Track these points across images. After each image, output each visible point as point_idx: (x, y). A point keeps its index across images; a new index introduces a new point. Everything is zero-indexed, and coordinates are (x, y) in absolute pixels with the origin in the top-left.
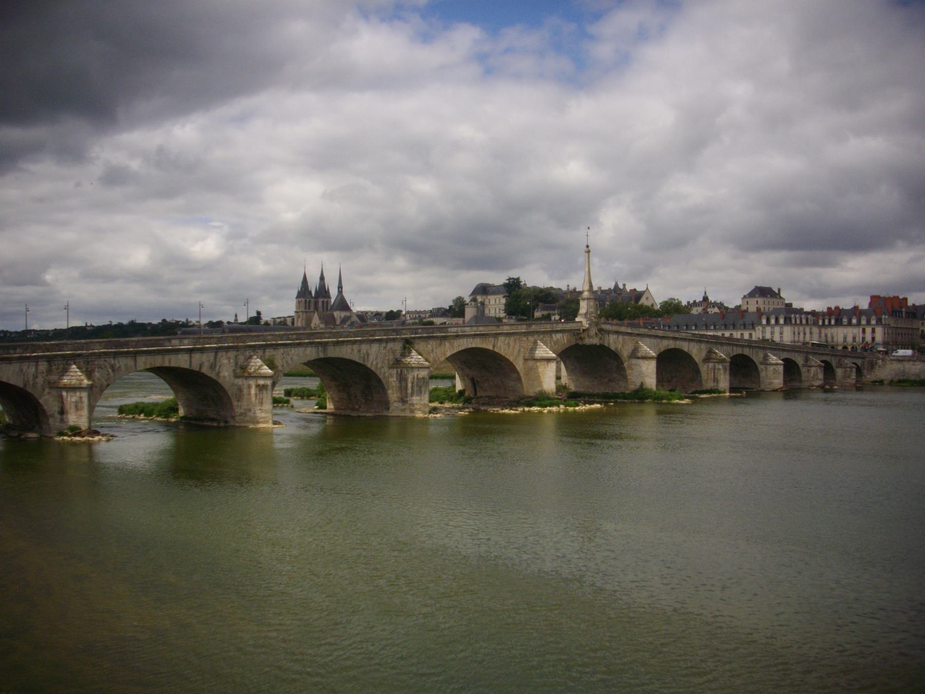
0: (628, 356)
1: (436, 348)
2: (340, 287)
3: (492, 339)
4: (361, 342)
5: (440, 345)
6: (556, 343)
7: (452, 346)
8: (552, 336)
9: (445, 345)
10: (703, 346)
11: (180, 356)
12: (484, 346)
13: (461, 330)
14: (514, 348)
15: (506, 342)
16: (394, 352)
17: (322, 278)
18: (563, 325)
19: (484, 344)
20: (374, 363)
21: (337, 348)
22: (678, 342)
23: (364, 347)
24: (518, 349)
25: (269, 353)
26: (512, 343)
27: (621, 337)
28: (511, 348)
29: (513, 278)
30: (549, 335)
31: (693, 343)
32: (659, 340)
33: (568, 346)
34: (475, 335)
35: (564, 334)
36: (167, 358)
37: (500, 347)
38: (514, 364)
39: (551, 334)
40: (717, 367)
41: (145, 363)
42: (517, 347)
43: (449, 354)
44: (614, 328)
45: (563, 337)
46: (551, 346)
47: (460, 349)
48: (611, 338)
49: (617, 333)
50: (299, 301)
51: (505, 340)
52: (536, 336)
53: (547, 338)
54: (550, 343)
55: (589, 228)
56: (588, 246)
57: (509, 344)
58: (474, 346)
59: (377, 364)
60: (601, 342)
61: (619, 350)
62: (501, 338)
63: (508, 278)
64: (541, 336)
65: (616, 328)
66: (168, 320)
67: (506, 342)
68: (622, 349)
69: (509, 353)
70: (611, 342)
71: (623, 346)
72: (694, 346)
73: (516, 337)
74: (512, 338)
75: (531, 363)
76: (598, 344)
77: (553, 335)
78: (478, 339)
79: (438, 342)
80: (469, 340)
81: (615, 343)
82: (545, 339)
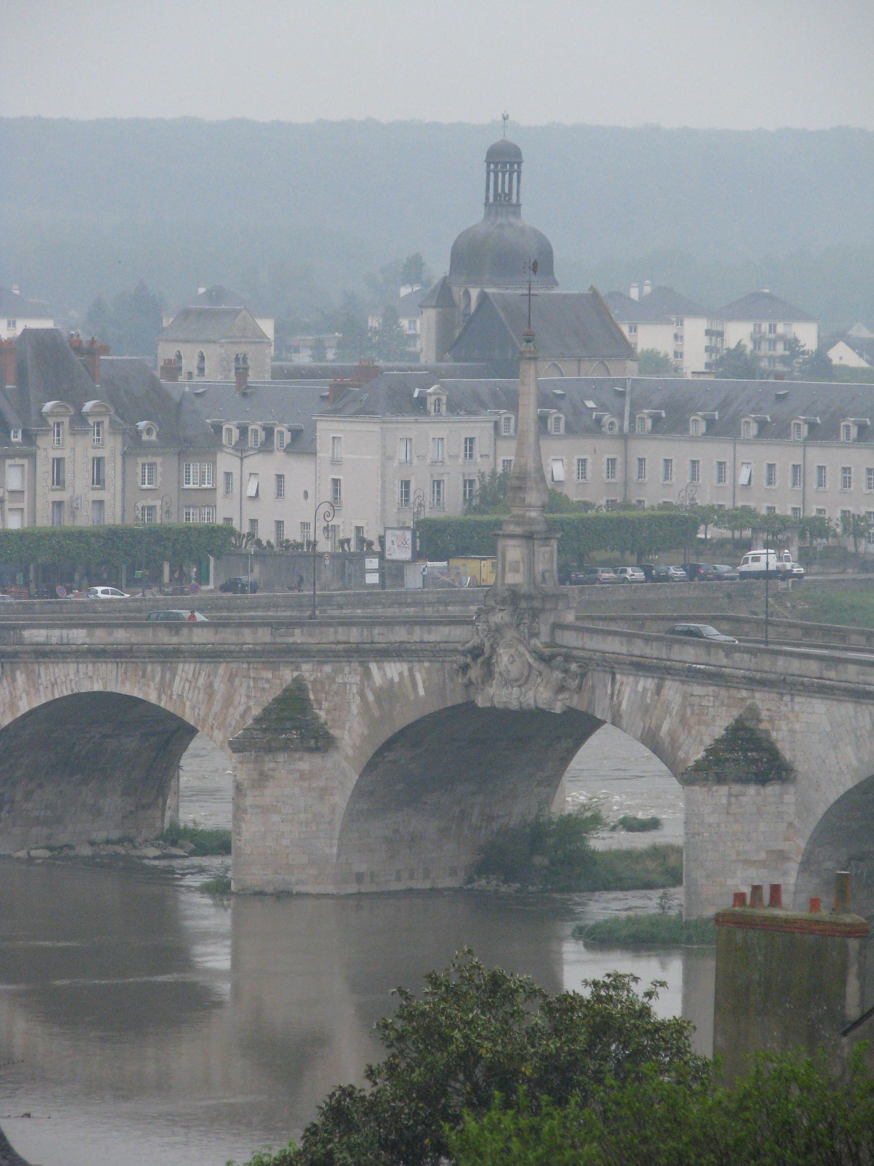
3: (155, 670)
6: (379, 694)
7: (33, 682)
9: (14, 680)
12: (130, 689)
13: (62, 638)
14: (228, 701)
15: (201, 681)
18: (410, 633)
19: (128, 684)
24: (242, 708)
26: (220, 687)
27: (672, 690)
30: (356, 665)
33: (431, 709)
34: (97, 654)
35: (417, 666)
37: (180, 696)
39: (364, 665)
43: (24, 707)
44: (639, 648)
45: (411, 670)
47: (57, 696)
48: (627, 690)
49: (640, 667)
51: (196, 676)
52: (307, 670)
58: (97, 687)
60: (576, 702)
61: (667, 740)
62: (185, 669)
64: (328, 669)
65: (648, 651)
67: (201, 681)
69: (210, 720)
70: (624, 706)
71: (683, 721)
73: (235, 665)
74: (222, 669)
76: (558, 709)
77: (373, 666)
78: (112, 667)
80: (82, 667)
81: (646, 710)
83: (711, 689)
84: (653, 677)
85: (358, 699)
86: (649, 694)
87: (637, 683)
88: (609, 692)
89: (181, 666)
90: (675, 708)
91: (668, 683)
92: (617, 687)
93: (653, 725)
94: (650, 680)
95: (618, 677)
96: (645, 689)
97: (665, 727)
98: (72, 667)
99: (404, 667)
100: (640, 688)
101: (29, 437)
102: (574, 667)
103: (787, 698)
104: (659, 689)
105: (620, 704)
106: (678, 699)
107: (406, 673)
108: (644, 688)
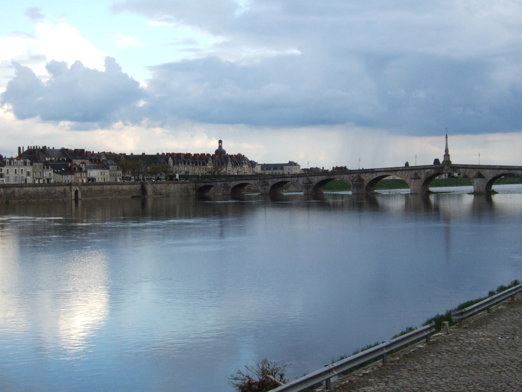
0: (473, 177)
1: (370, 176)
4: (341, 174)
5: (371, 175)
8: (425, 171)
11: (289, 179)
14: (405, 175)
16: (353, 177)
20: (346, 180)
21: (333, 176)
22: (512, 171)
23: (342, 176)
25: (313, 177)
26: (404, 174)
27: (468, 170)
28: (403, 175)
32: (496, 171)
36: (286, 179)
38: (405, 180)
41: (280, 180)
42: (406, 174)
43: (375, 177)
45: (431, 170)
46: (425, 174)
52: (416, 171)
53: (423, 171)
54: (424, 173)
57: (402, 174)
59: (347, 180)
64: (419, 171)
66: (338, 166)
67: (401, 173)
68: (469, 174)
71: (469, 173)
74: (404, 171)
75: (411, 180)
77: (426, 170)
79: (370, 173)
80: (383, 173)
82: (421, 172)
85: (423, 173)
89: (398, 172)
98: (382, 173)
99: (430, 170)
101: (242, 165)
102: (454, 168)
104: (466, 170)
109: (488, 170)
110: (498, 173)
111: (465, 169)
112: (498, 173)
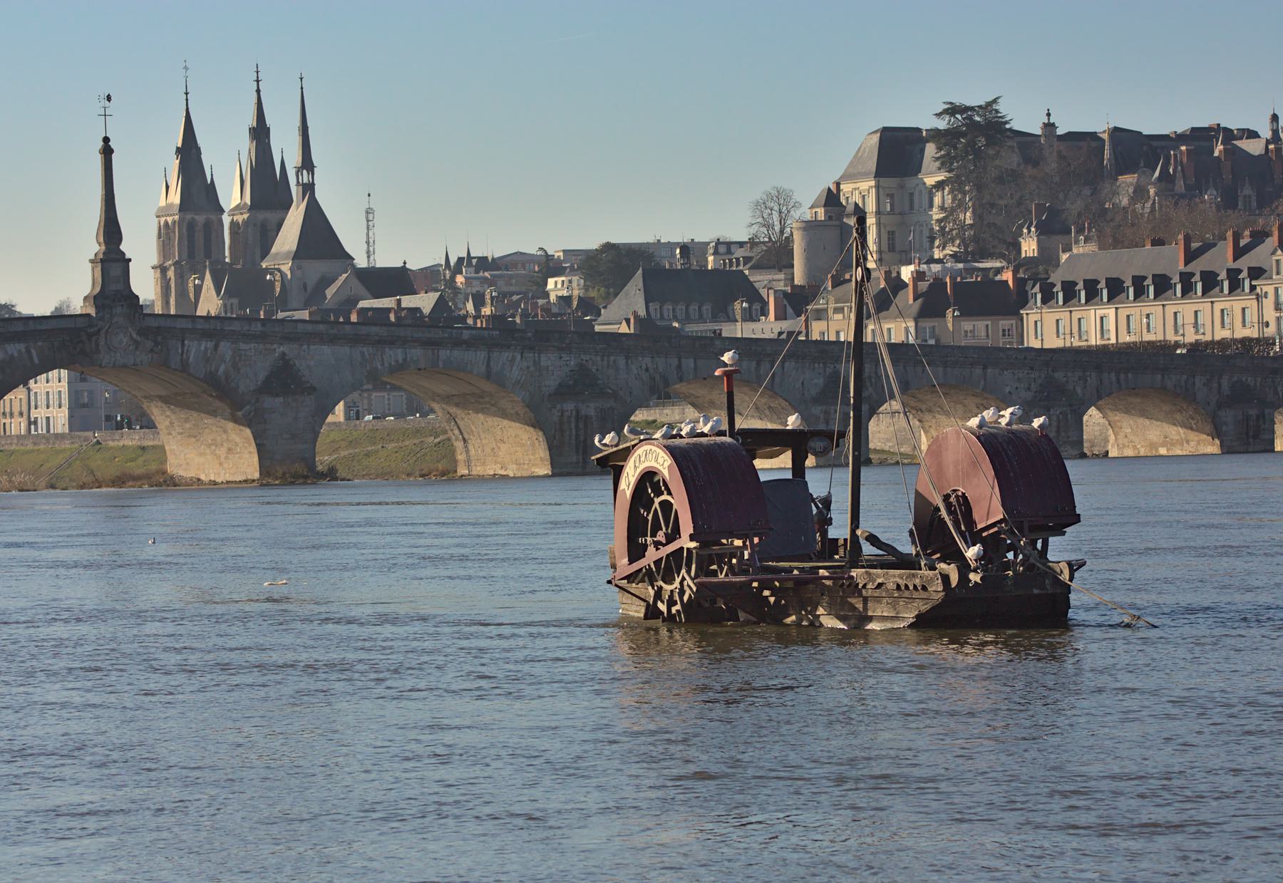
2: (307, 164)
10: (549, 360)
17: (260, 133)
27: (225, 348)
29: (964, 109)
31: (506, 355)
40: (583, 413)
48: (194, 350)
50: (166, 223)
55: (109, 98)
56: (106, 140)
63: (947, 106)
70: (191, 359)
72: (512, 361)
83: (252, 345)
84: (211, 341)
86: (209, 351)
87: (201, 345)
88: (180, 351)
90: (228, 358)
91: (222, 344)
92: (186, 348)
93: (213, 369)
94: (209, 343)
95: (186, 342)
96: (206, 349)
97: (222, 368)
99: (22, 347)
100: (203, 348)
103: (305, 347)
105: (189, 358)
106: (230, 352)
107: (23, 350)
108: (206, 348)
109: (327, 350)
110: (380, 367)
111: (210, 345)
112: (380, 367)
